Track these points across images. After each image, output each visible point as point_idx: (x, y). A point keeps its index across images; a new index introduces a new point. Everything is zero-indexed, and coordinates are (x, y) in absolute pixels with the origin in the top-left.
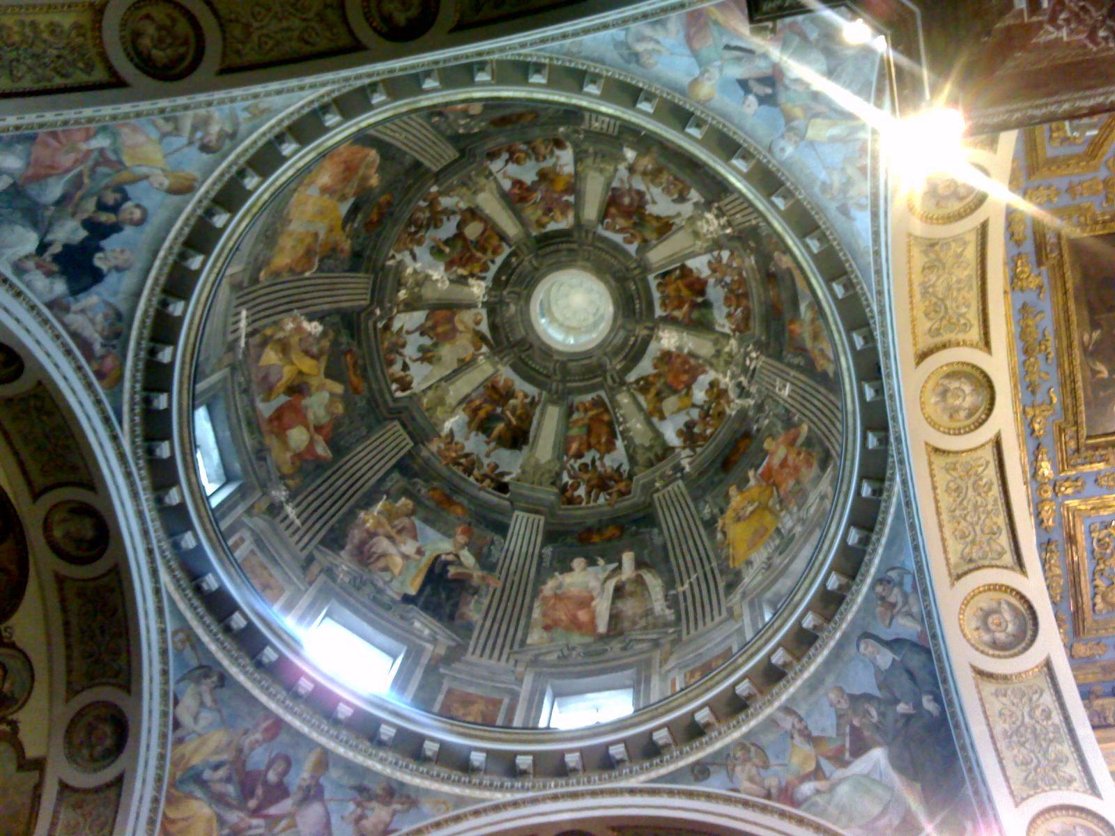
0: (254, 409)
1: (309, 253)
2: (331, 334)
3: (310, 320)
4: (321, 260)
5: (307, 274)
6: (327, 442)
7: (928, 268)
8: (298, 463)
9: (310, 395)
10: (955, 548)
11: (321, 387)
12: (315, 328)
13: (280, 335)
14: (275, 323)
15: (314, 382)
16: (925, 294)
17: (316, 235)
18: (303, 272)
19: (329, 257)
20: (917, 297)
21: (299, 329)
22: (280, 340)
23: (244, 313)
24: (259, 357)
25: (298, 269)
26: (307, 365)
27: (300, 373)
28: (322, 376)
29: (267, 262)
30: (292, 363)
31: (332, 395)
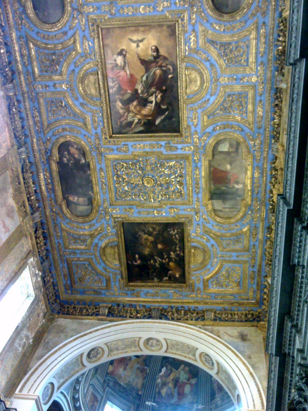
0: (173, 405)
1: (142, 371)
2: (167, 364)
3: (160, 371)
4: (146, 366)
5: (148, 371)
6: (193, 378)
7: (117, 349)
8: (192, 393)
9: (179, 378)
10: (190, 356)
11: (179, 373)
12: (164, 370)
13: (160, 385)
14: (156, 387)
15: (177, 375)
16: (124, 349)
17: (138, 368)
18: (147, 373)
19: (146, 362)
20: (125, 351)
21: (162, 377)
22: (161, 386)
23: (147, 403)
24: (162, 396)
25: (145, 375)
26: (172, 377)
27: (173, 380)
28: (176, 371)
29: (138, 390)
30: (169, 382)
31: (183, 370)
